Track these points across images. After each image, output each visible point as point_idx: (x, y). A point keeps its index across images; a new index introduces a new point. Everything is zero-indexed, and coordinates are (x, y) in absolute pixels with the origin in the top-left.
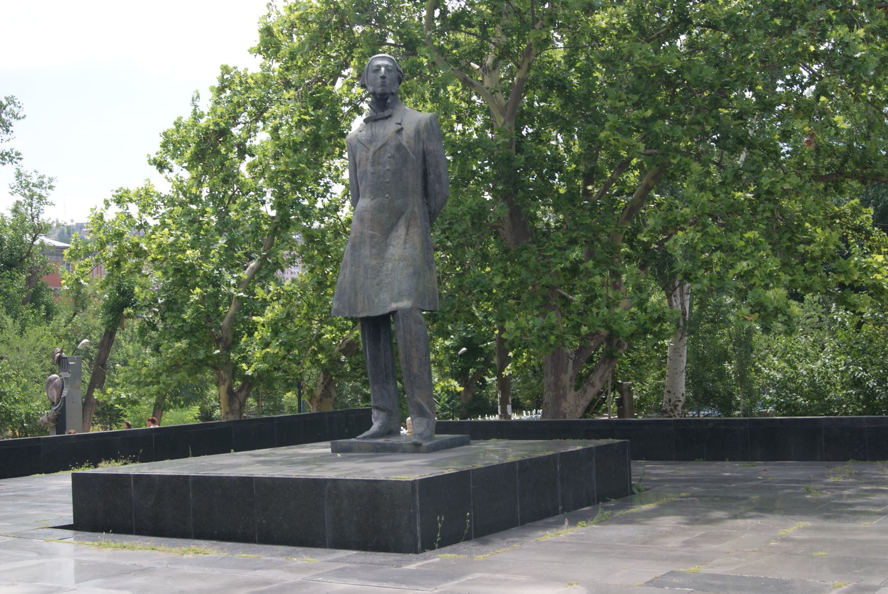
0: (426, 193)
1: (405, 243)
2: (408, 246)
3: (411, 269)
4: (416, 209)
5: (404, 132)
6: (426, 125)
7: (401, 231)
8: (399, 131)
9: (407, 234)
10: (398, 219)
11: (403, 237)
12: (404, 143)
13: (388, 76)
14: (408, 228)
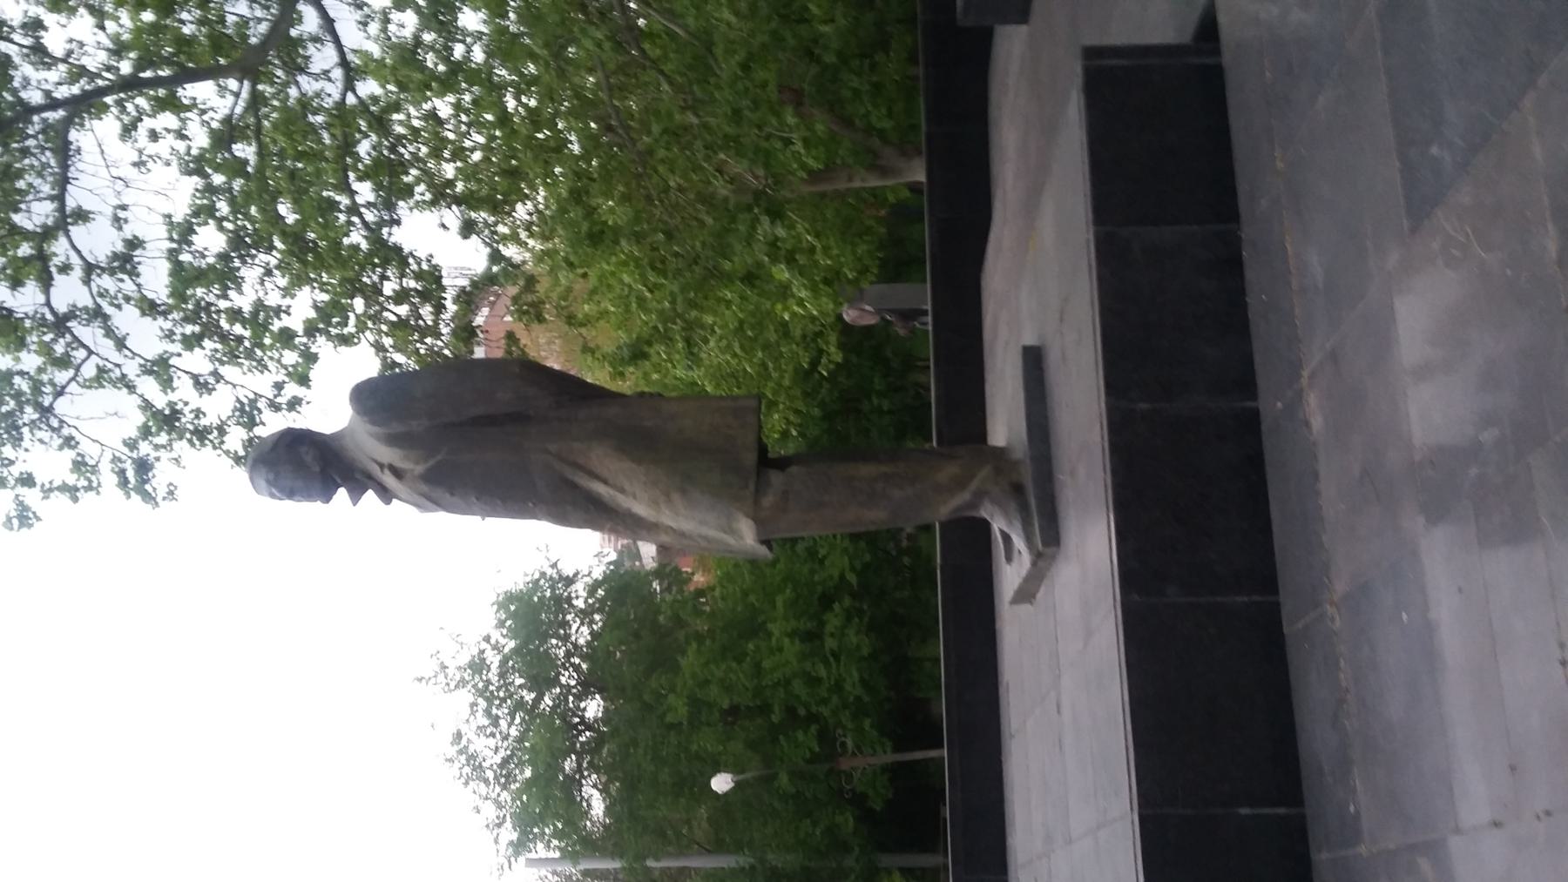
0: (518, 418)
1: (622, 491)
2: (627, 487)
3: (676, 497)
4: (553, 447)
5: (399, 464)
6: (373, 423)
8: (397, 473)
9: (605, 482)
10: (574, 486)
11: (612, 492)
12: (420, 469)
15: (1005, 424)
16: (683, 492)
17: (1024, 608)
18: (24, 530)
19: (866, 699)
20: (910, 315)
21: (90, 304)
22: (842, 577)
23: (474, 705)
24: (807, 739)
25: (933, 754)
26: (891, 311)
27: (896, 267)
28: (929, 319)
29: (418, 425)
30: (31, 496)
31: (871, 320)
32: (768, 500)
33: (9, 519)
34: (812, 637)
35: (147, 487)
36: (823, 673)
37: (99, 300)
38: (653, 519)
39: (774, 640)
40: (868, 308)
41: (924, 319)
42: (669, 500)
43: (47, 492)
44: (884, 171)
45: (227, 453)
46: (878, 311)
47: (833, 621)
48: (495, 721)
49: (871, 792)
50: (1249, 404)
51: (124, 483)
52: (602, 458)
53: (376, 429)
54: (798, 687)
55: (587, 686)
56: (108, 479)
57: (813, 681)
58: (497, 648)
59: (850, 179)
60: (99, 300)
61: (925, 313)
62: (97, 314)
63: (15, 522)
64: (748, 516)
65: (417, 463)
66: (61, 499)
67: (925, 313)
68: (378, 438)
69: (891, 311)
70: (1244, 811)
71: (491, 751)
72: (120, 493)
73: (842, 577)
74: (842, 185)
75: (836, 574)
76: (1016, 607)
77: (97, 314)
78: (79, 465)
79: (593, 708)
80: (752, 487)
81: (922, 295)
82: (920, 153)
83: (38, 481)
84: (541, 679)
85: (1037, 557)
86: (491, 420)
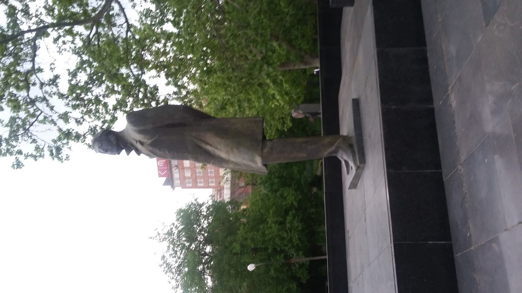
1: (217, 148)
2: (218, 147)
3: (235, 150)
4: (194, 134)
5: (143, 140)
7: (209, 148)
8: (142, 143)
9: (211, 145)
10: (200, 148)
11: (213, 149)
12: (149, 142)
13: (105, 147)
14: (207, 143)
15: (346, 127)
16: (237, 148)
17: (353, 191)
18: (19, 169)
19: (300, 245)
20: (315, 114)
21: (41, 95)
22: (292, 203)
23: (169, 247)
24: (280, 258)
25: (323, 257)
26: (308, 113)
27: (310, 99)
28: (321, 116)
29: (149, 126)
30: (21, 158)
31: (301, 116)
32: (266, 150)
33: (13, 165)
34: (282, 223)
35: (60, 156)
36: (286, 236)
37: (45, 95)
38: (227, 159)
39: (269, 225)
40: (301, 112)
41: (319, 116)
42: (232, 151)
43: (27, 156)
44: (306, 63)
45: (86, 144)
46: (304, 113)
47: (289, 218)
48: (176, 252)
49: (302, 277)
50: (431, 106)
51: (52, 154)
52: (210, 138)
53: (134, 128)
54: (277, 240)
55: (207, 241)
56: (47, 153)
57: (283, 239)
58: (176, 227)
59: (294, 66)
60: (45, 95)
61: (320, 114)
62: (44, 99)
63: (16, 166)
64: (259, 155)
65: (148, 140)
66: (31, 160)
67: (320, 114)
68: (135, 131)
69: (308, 113)
70: (430, 242)
71: (174, 263)
72: (50, 158)
73: (292, 203)
74: (292, 68)
75: (290, 203)
76: (350, 190)
77: (44, 99)
78: (37, 148)
79: (208, 249)
80: (260, 146)
81: (319, 108)
82: (317, 57)
83: (23, 153)
84: (191, 239)
85: (358, 168)
86: (173, 125)
